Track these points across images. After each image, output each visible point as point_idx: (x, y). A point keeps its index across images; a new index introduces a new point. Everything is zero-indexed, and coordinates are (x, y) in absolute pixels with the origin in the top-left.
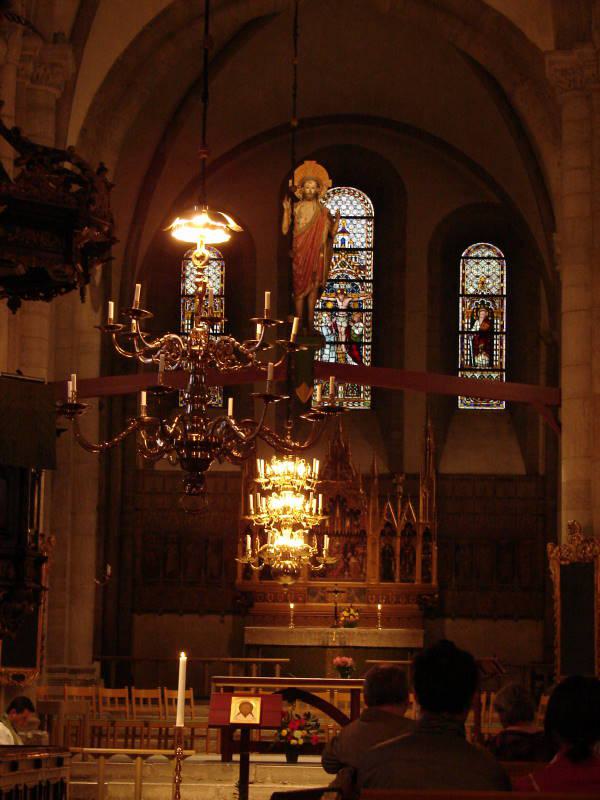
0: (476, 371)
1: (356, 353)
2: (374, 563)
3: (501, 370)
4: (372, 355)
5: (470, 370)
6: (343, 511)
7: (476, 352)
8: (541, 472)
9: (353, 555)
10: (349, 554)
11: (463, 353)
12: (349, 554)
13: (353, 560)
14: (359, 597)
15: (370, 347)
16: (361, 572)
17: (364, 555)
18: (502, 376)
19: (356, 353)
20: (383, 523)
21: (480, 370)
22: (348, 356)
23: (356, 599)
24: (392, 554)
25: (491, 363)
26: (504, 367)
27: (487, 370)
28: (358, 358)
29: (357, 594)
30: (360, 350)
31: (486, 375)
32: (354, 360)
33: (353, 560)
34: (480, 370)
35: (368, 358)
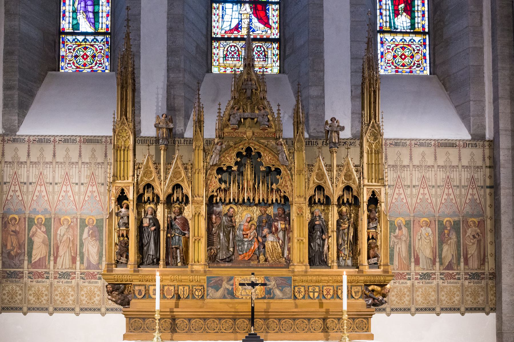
0: (396, 33)
1: (262, 14)
2: (300, 241)
3: (424, 33)
4: (281, 16)
5: (390, 32)
6: (256, 173)
7: (397, 13)
8: (489, 135)
9: (271, 232)
10: (266, 231)
11: (381, 14)
12: (266, 231)
13: (270, 238)
14: (281, 291)
15: (277, 6)
16: (283, 255)
17: (287, 231)
18: (424, 40)
19: (262, 14)
20: (311, 185)
21: (401, 32)
22: (253, 17)
23: (278, 292)
24: (324, 230)
25: (413, 25)
26: (427, 30)
27: (409, 33)
28: (265, 21)
29: (278, 286)
30: (265, 10)
31: (407, 38)
32: (260, 20)
33: (270, 238)
34: (401, 32)
35: (276, 19)
